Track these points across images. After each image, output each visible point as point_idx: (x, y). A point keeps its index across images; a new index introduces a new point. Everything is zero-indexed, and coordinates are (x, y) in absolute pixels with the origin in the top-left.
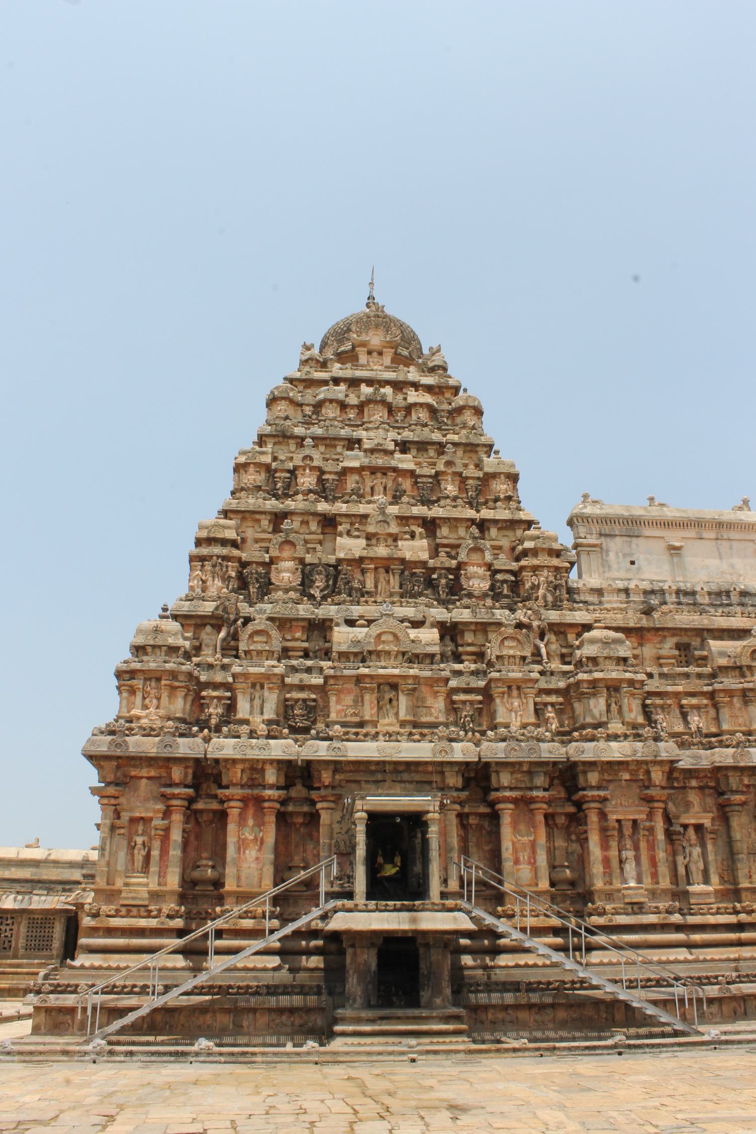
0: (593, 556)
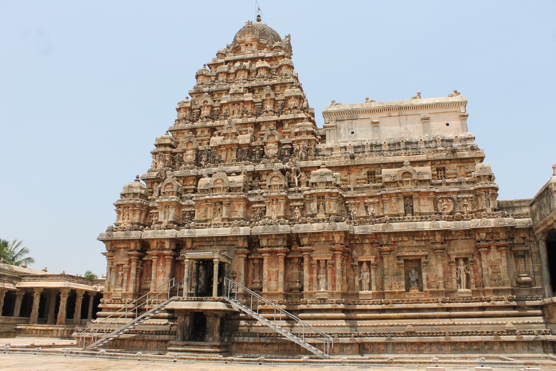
0: (332, 131)
